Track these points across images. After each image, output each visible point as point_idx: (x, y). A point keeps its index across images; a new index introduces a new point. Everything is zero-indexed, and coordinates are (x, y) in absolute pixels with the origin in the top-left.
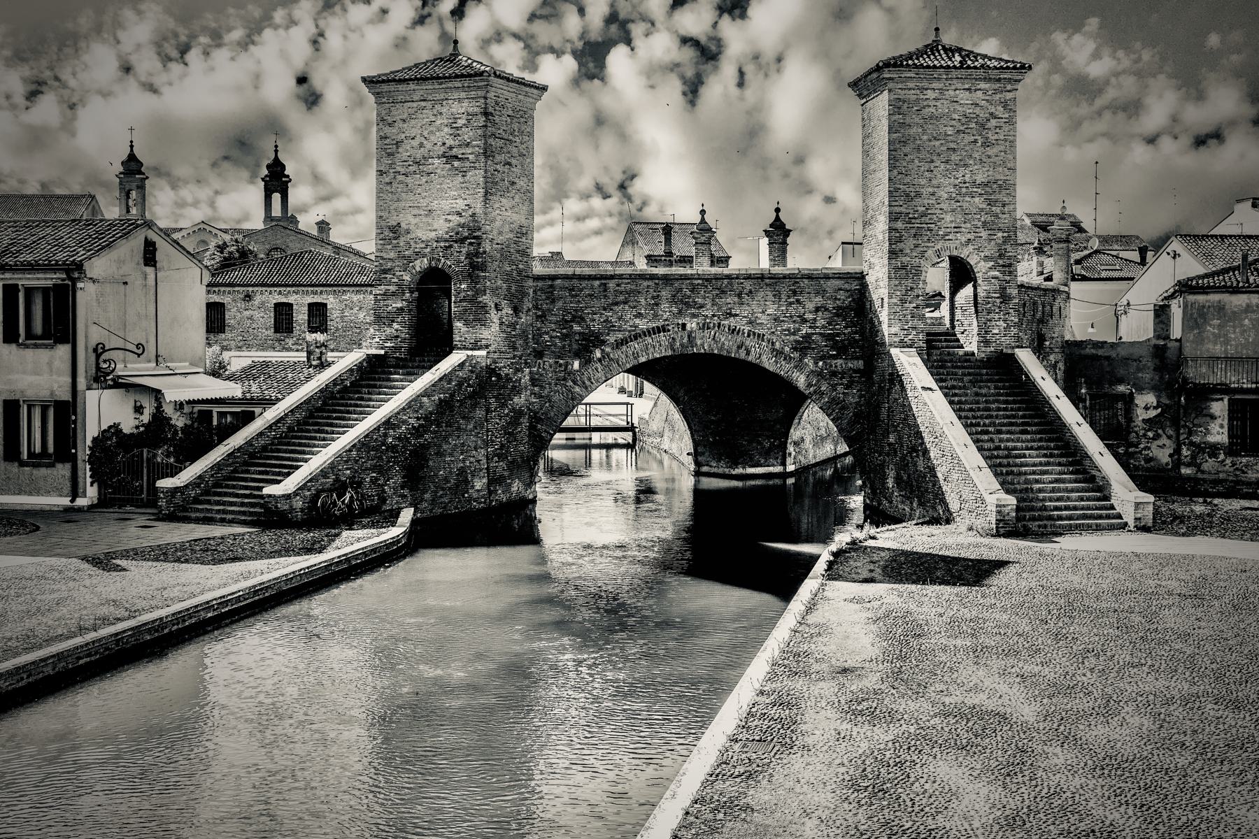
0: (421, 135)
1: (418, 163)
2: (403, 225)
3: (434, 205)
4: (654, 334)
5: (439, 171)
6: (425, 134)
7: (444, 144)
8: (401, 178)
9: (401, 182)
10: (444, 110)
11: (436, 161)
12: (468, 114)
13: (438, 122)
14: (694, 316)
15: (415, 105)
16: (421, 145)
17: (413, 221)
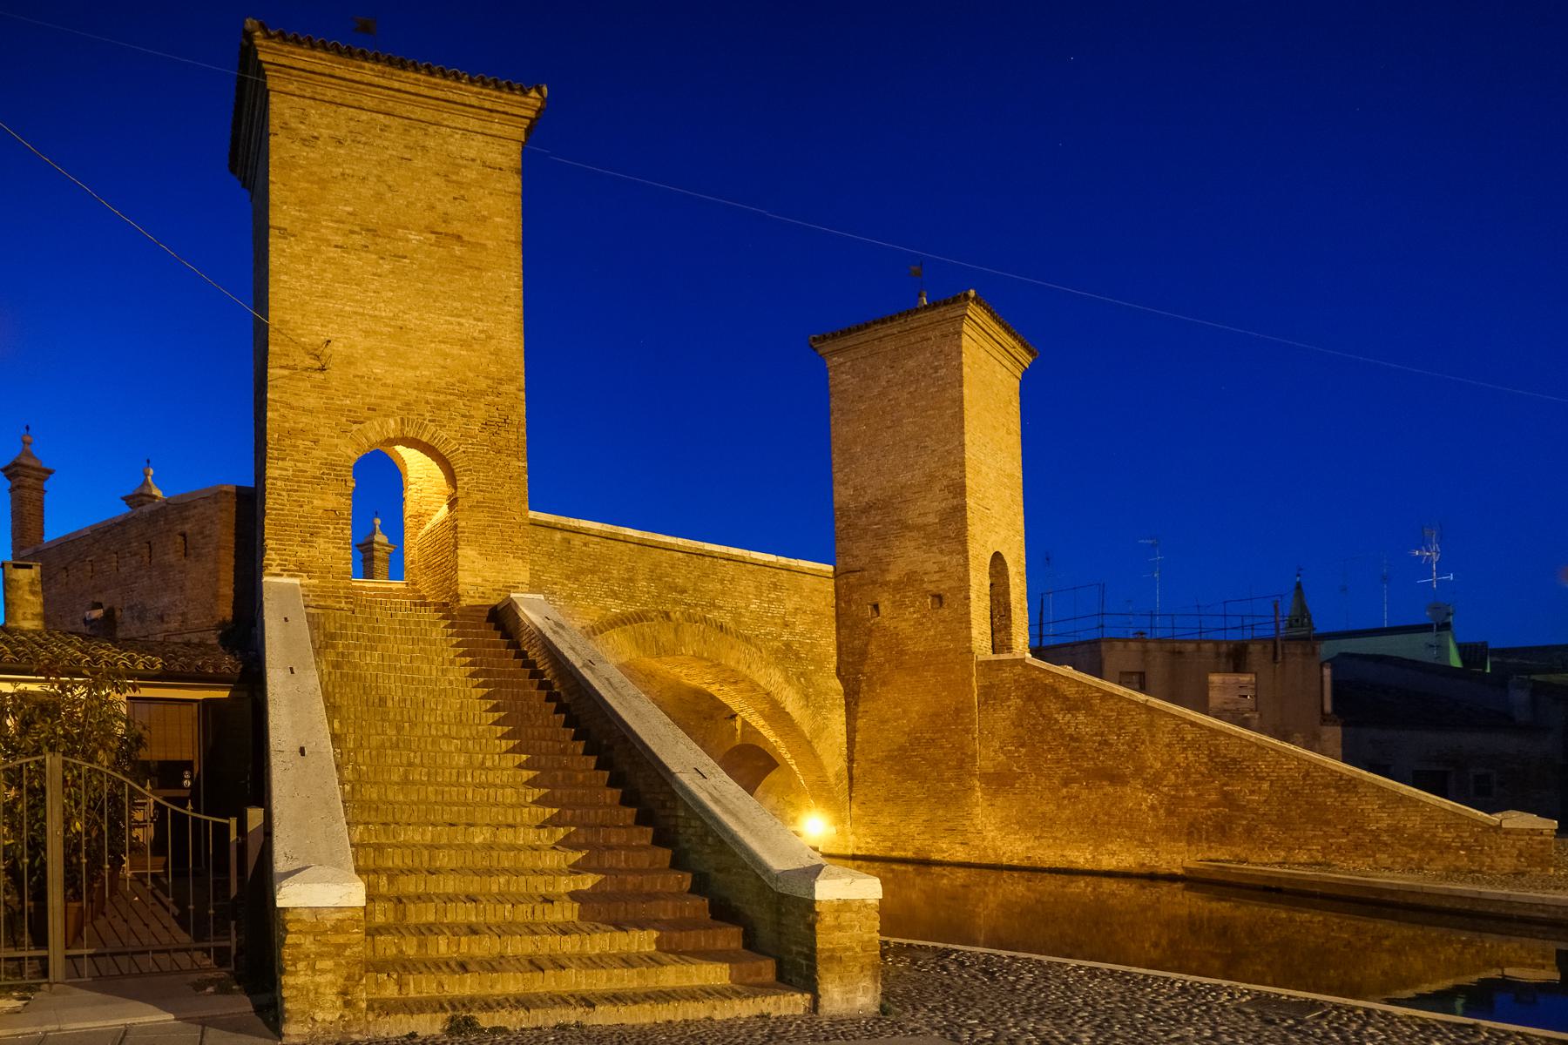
0: (379, 177)
1: (373, 232)
2: (338, 346)
3: (412, 319)
4: (631, 623)
5: (420, 256)
6: (389, 178)
7: (432, 208)
8: (334, 253)
9: (329, 260)
10: (430, 143)
11: (413, 236)
12: (484, 164)
13: (418, 163)
14: (676, 602)
15: (365, 116)
16: (379, 198)
17: (359, 339)
